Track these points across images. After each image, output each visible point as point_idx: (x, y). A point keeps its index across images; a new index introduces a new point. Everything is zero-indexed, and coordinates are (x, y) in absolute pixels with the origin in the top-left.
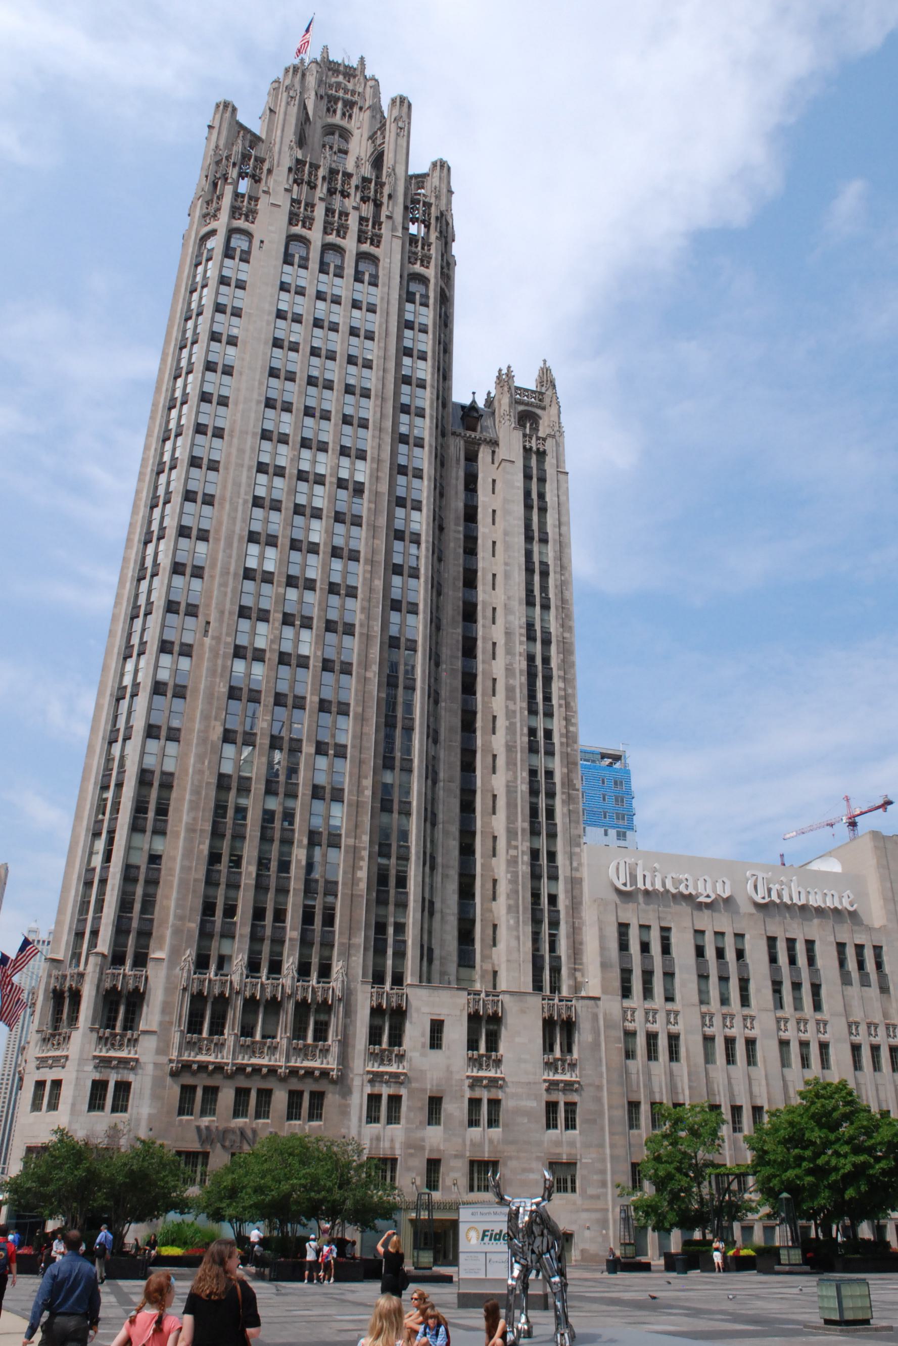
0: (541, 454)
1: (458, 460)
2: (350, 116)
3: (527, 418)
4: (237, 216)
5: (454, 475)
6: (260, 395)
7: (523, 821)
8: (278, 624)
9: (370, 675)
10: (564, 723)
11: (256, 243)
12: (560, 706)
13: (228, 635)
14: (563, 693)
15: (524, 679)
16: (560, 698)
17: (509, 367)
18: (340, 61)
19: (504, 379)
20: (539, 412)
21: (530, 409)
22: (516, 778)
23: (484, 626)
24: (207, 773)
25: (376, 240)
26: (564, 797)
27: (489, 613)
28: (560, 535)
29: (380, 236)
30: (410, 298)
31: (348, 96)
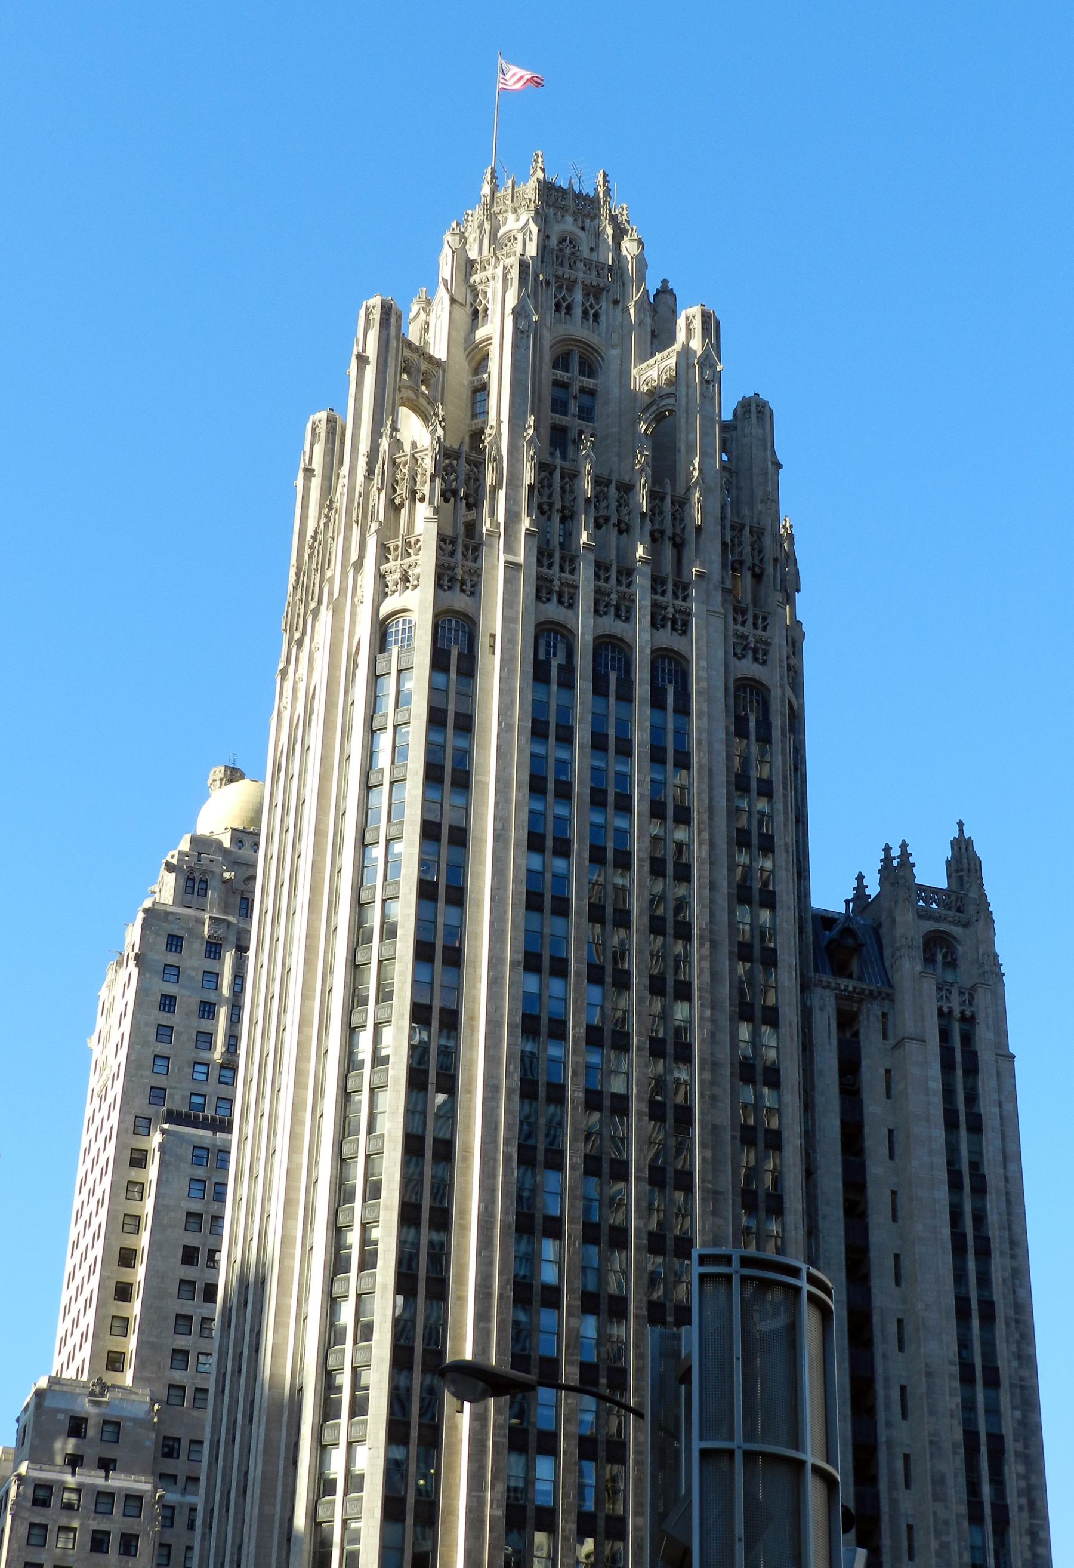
0: (968, 1021)
2: (596, 316)
3: (938, 948)
10: (1027, 1540)
12: (1021, 1508)
14: (1023, 1484)
15: (959, 1461)
16: (1020, 1493)
17: (904, 846)
18: (566, 186)
19: (897, 869)
20: (957, 931)
21: (942, 926)
25: (681, 624)
27: (893, 1328)
28: (1006, 1180)
29: (688, 613)
31: (593, 279)
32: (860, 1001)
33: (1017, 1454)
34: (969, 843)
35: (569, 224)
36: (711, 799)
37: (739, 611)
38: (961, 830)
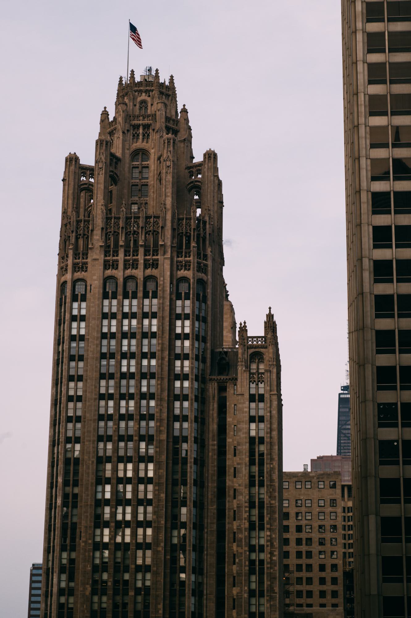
1: (214, 397)
4: (77, 270)
5: (211, 408)
6: (95, 395)
7: (245, 614)
8: (112, 529)
9: (160, 549)
10: (269, 556)
11: (88, 288)
13: (90, 539)
17: (245, 323)
20: (262, 350)
21: (257, 350)
22: (242, 591)
23: (229, 501)
24: (86, 612)
25: (155, 265)
26: (268, 598)
30: (179, 297)
31: (146, 122)
32: (227, 382)
33: (267, 529)
34: (273, 315)
35: (144, 97)
36: (163, 328)
37: (179, 254)
38: (270, 311)
